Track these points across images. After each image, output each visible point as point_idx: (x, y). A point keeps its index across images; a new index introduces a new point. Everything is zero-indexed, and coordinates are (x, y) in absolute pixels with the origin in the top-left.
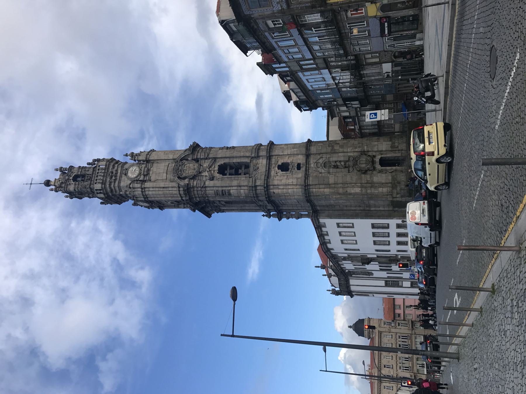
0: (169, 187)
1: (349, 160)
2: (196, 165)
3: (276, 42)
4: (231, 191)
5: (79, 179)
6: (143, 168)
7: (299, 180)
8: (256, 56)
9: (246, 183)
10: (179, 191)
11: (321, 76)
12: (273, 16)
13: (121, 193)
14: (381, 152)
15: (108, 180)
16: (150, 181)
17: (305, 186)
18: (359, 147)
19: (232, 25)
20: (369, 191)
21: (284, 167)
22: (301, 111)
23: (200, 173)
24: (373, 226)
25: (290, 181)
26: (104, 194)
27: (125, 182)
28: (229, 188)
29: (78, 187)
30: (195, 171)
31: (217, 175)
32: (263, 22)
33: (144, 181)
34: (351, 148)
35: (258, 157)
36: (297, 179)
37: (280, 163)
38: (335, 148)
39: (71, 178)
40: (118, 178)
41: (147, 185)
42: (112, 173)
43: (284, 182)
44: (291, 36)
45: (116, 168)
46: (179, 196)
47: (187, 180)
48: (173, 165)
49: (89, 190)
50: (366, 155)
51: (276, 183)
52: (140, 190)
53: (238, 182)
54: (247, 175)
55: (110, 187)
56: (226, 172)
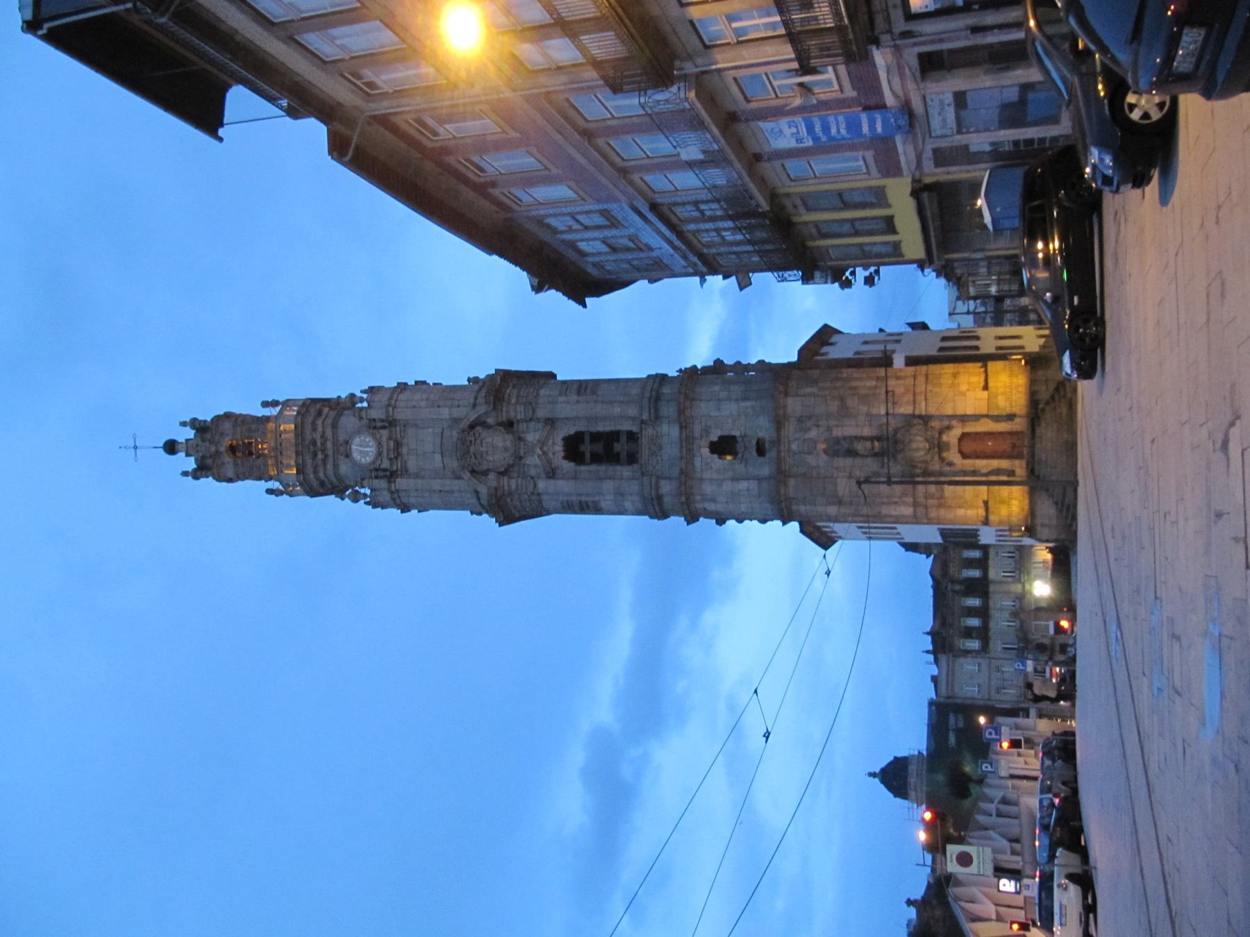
0: (452, 492)
2: (509, 437)
4: (603, 505)
6: (384, 439)
10: (478, 498)
15: (309, 461)
16: (404, 472)
21: (724, 446)
23: (521, 458)
28: (596, 498)
30: (507, 455)
33: (391, 476)
35: (657, 417)
36: (759, 479)
39: (223, 449)
40: (330, 452)
41: (401, 483)
42: (314, 443)
45: (320, 429)
47: (492, 476)
51: (708, 489)
54: (636, 466)
55: (318, 479)
56: (582, 448)
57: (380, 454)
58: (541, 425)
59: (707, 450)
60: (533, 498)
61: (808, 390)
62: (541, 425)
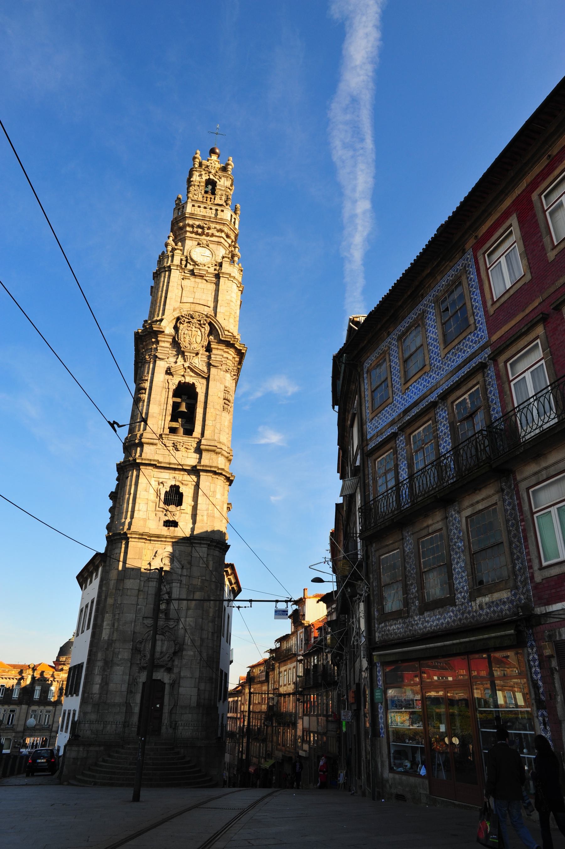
1: (167, 618)
5: (210, 187)
7: (142, 523)
14: (175, 684)
15: (197, 223)
18: (193, 641)
20: (100, 655)
21: (174, 497)
24: (80, 666)
31: (175, 381)
34: (193, 624)
42: (209, 228)
45: (218, 234)
50: (175, 653)
53: (155, 415)
54: (167, 431)
61: (211, 563)
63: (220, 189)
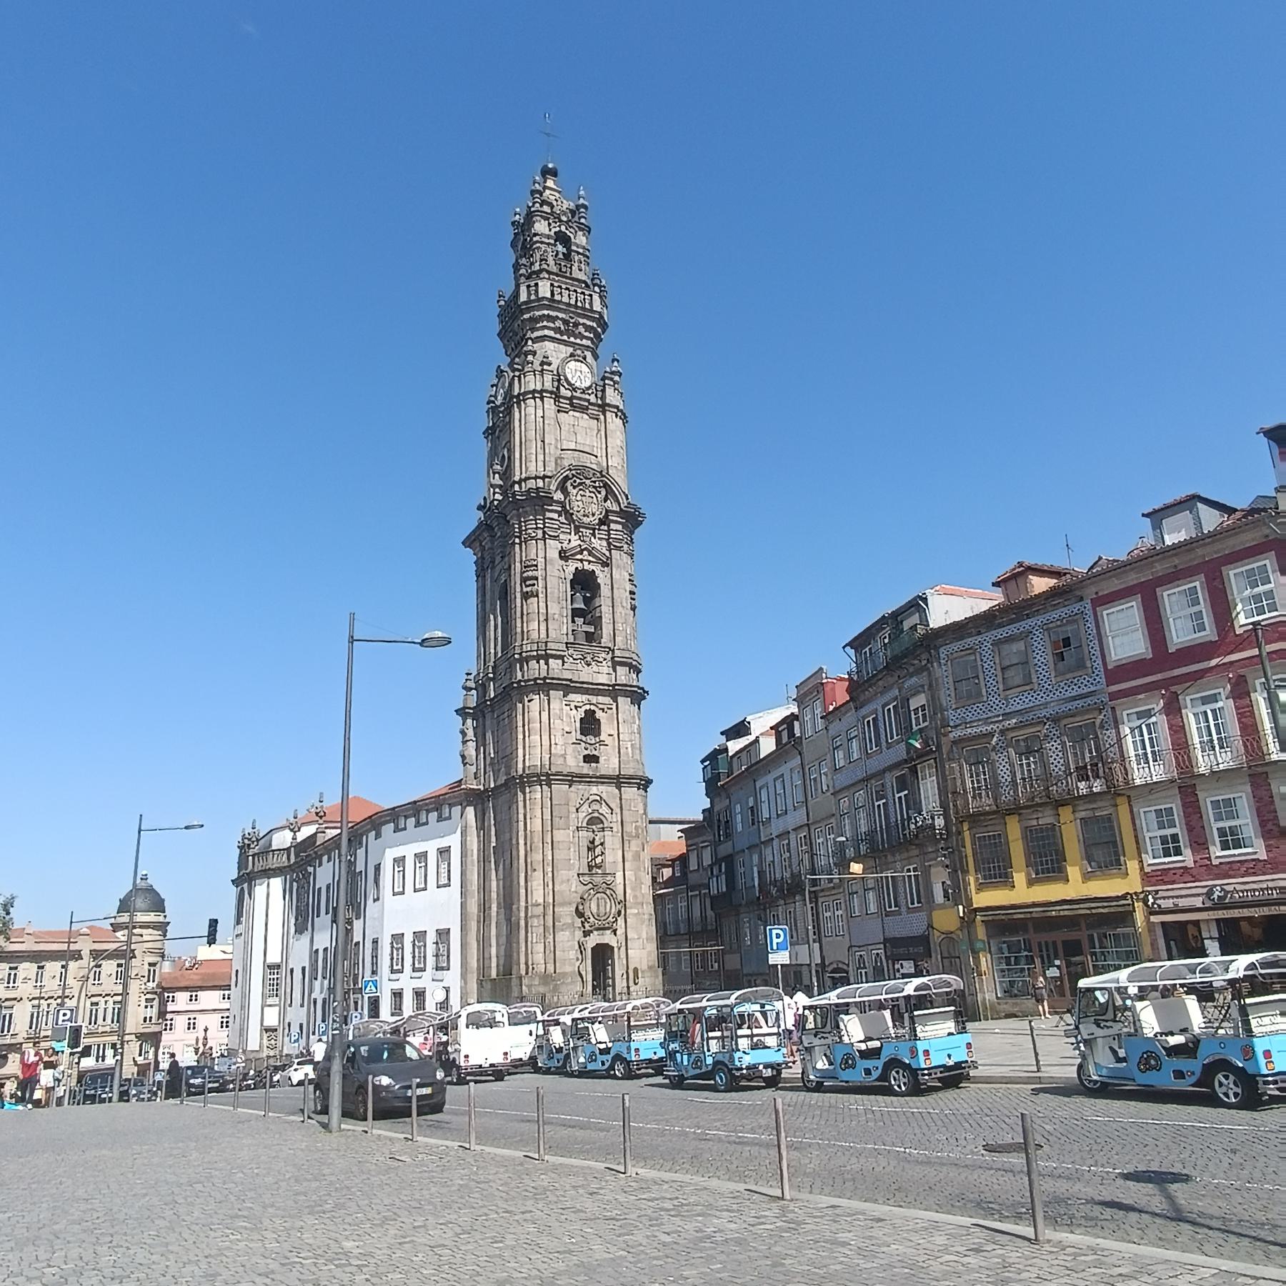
2: (594, 520)
3: (875, 711)
5: (560, 248)
7: (560, 761)
8: (840, 666)
9: (552, 634)
10: (536, 478)
11: (790, 807)
12: (935, 707)
13: (530, 342)
15: (561, 315)
17: (547, 775)
18: (635, 897)
19: (915, 619)
21: (590, 725)
22: (702, 762)
24: (443, 934)
25: (558, 739)
26: (525, 303)
27: (555, 352)
29: (542, 243)
32: (923, 686)
33: (557, 396)
35: (615, 664)
36: (564, 756)
37: (599, 714)
38: (633, 842)
39: (563, 228)
42: (576, 325)
43: (557, 723)
44: (889, 746)
45: (587, 334)
46: (523, 476)
48: (594, 467)
49: (536, 267)
50: (619, 913)
51: (555, 705)
52: (539, 388)
57: (574, 390)
58: (604, 551)
59: (588, 707)
60: (540, 533)
62: (604, 551)
63: (578, 253)
